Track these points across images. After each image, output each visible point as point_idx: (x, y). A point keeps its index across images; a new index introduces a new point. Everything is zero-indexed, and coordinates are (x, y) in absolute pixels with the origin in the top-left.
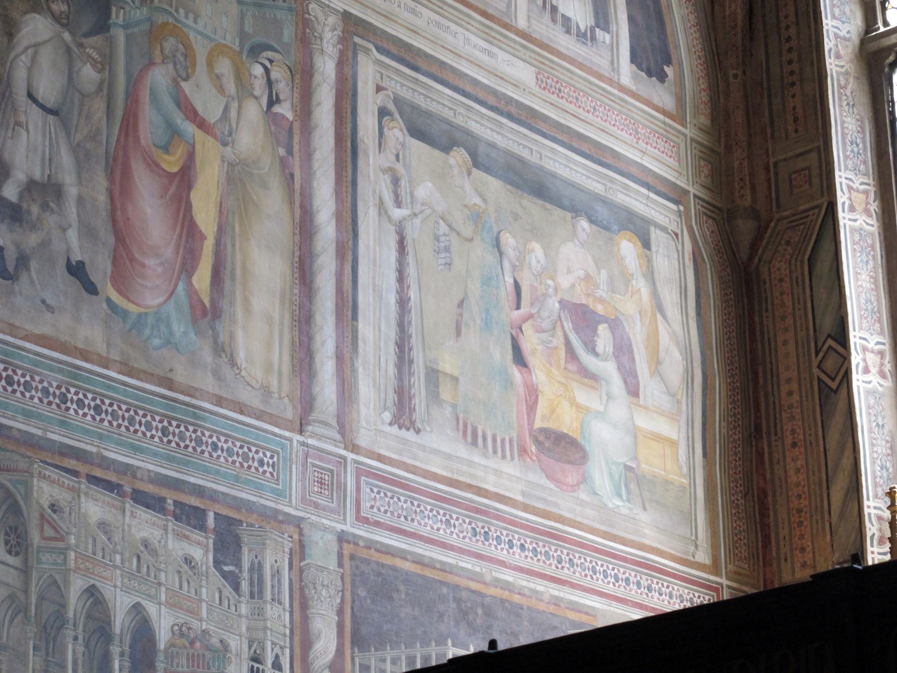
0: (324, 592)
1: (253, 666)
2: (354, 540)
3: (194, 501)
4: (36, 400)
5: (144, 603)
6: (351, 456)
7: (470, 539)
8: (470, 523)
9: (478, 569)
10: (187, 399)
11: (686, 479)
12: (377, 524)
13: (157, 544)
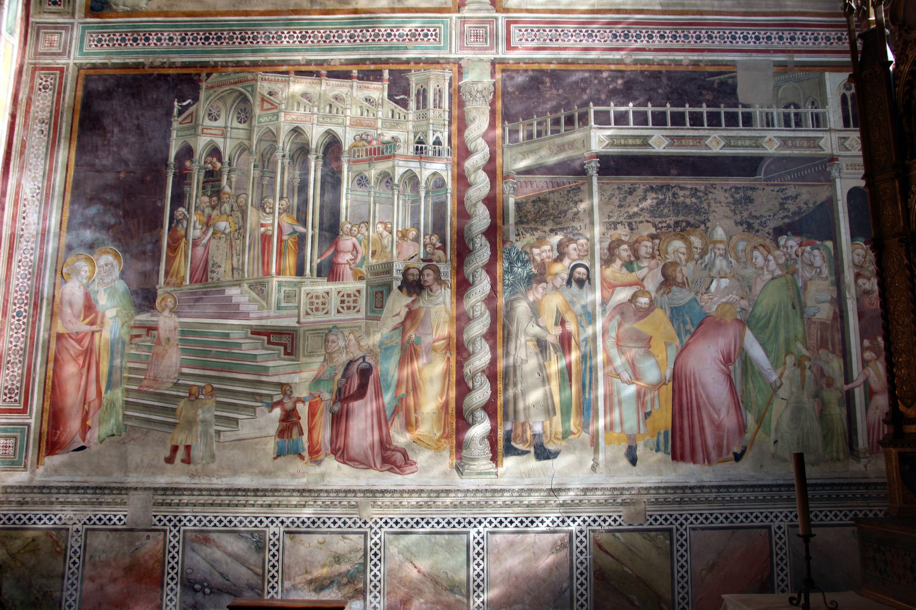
0: (478, 95)
1: (417, 147)
2: (502, 62)
3: (372, 67)
4: (261, 43)
5: (333, 128)
6: (500, 16)
10: (368, 15)
13: (344, 95)
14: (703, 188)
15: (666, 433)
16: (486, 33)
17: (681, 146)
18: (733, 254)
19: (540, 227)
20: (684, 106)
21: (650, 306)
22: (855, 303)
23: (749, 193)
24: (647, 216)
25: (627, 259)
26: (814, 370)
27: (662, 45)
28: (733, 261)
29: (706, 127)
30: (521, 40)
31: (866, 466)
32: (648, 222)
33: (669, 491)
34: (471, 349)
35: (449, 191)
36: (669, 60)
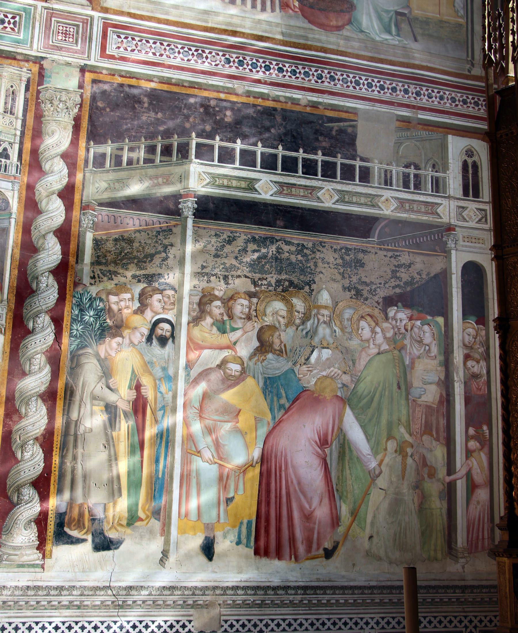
7: (223, 66)
8: (224, 55)
9: (230, 85)
11: (463, 19)
12: (123, 59)
14: (310, 245)
15: (249, 523)
16: (77, 33)
17: (290, 195)
18: (338, 323)
19: (121, 271)
20: (297, 151)
21: (241, 374)
22: (463, 386)
23: (361, 256)
24: (246, 270)
25: (219, 318)
26: (417, 458)
27: (280, 80)
28: (337, 330)
29: (319, 177)
30: (119, 48)
31: (463, 567)
32: (246, 277)
33: (249, 592)
34: (23, 410)
35: (14, 216)
36: (285, 97)
